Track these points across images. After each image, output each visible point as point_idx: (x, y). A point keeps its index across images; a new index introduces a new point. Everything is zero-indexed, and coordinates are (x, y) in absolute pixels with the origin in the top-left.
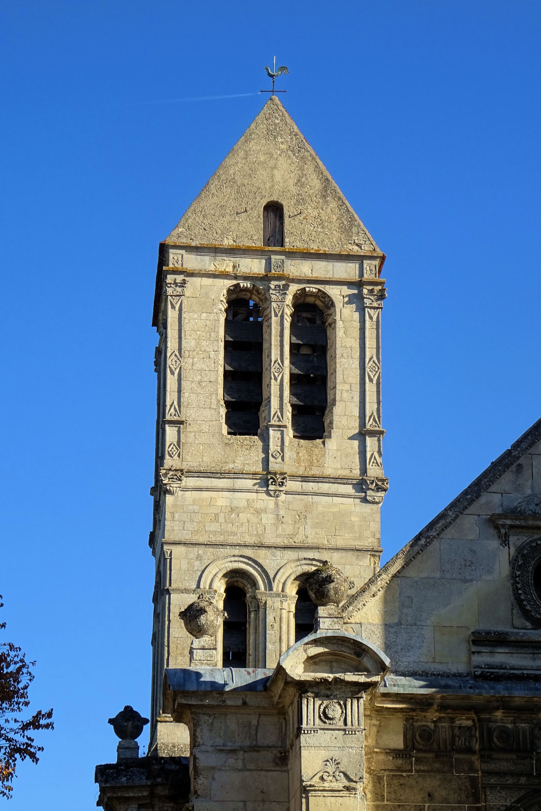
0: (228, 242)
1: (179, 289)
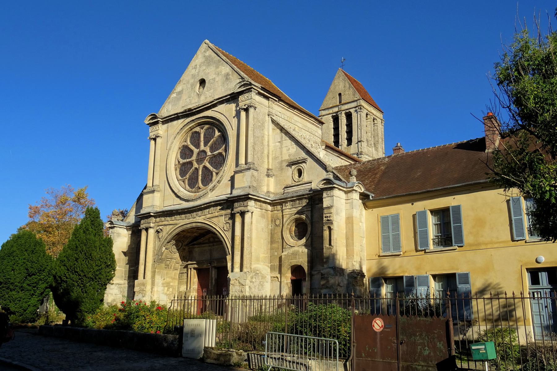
0: (331, 106)
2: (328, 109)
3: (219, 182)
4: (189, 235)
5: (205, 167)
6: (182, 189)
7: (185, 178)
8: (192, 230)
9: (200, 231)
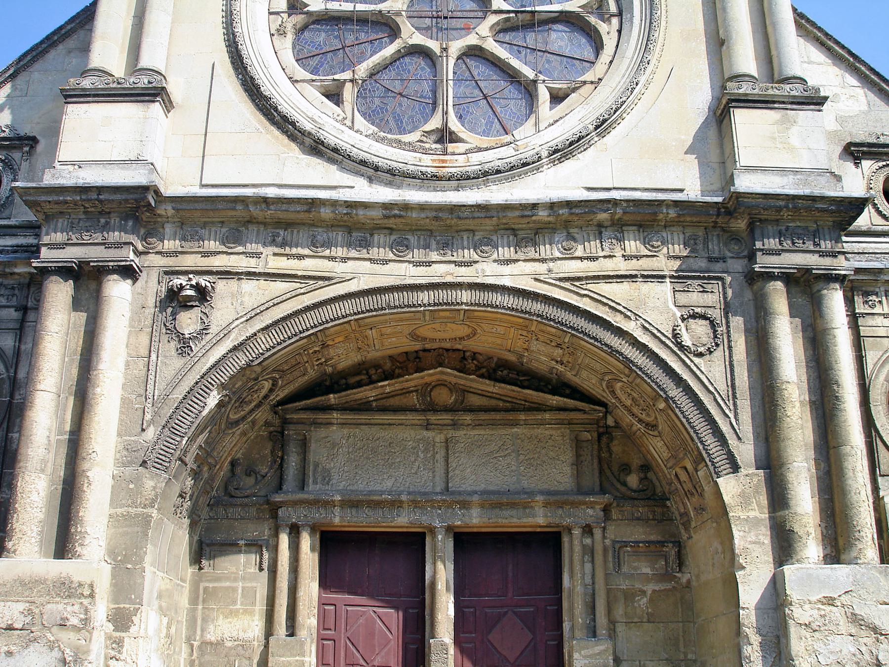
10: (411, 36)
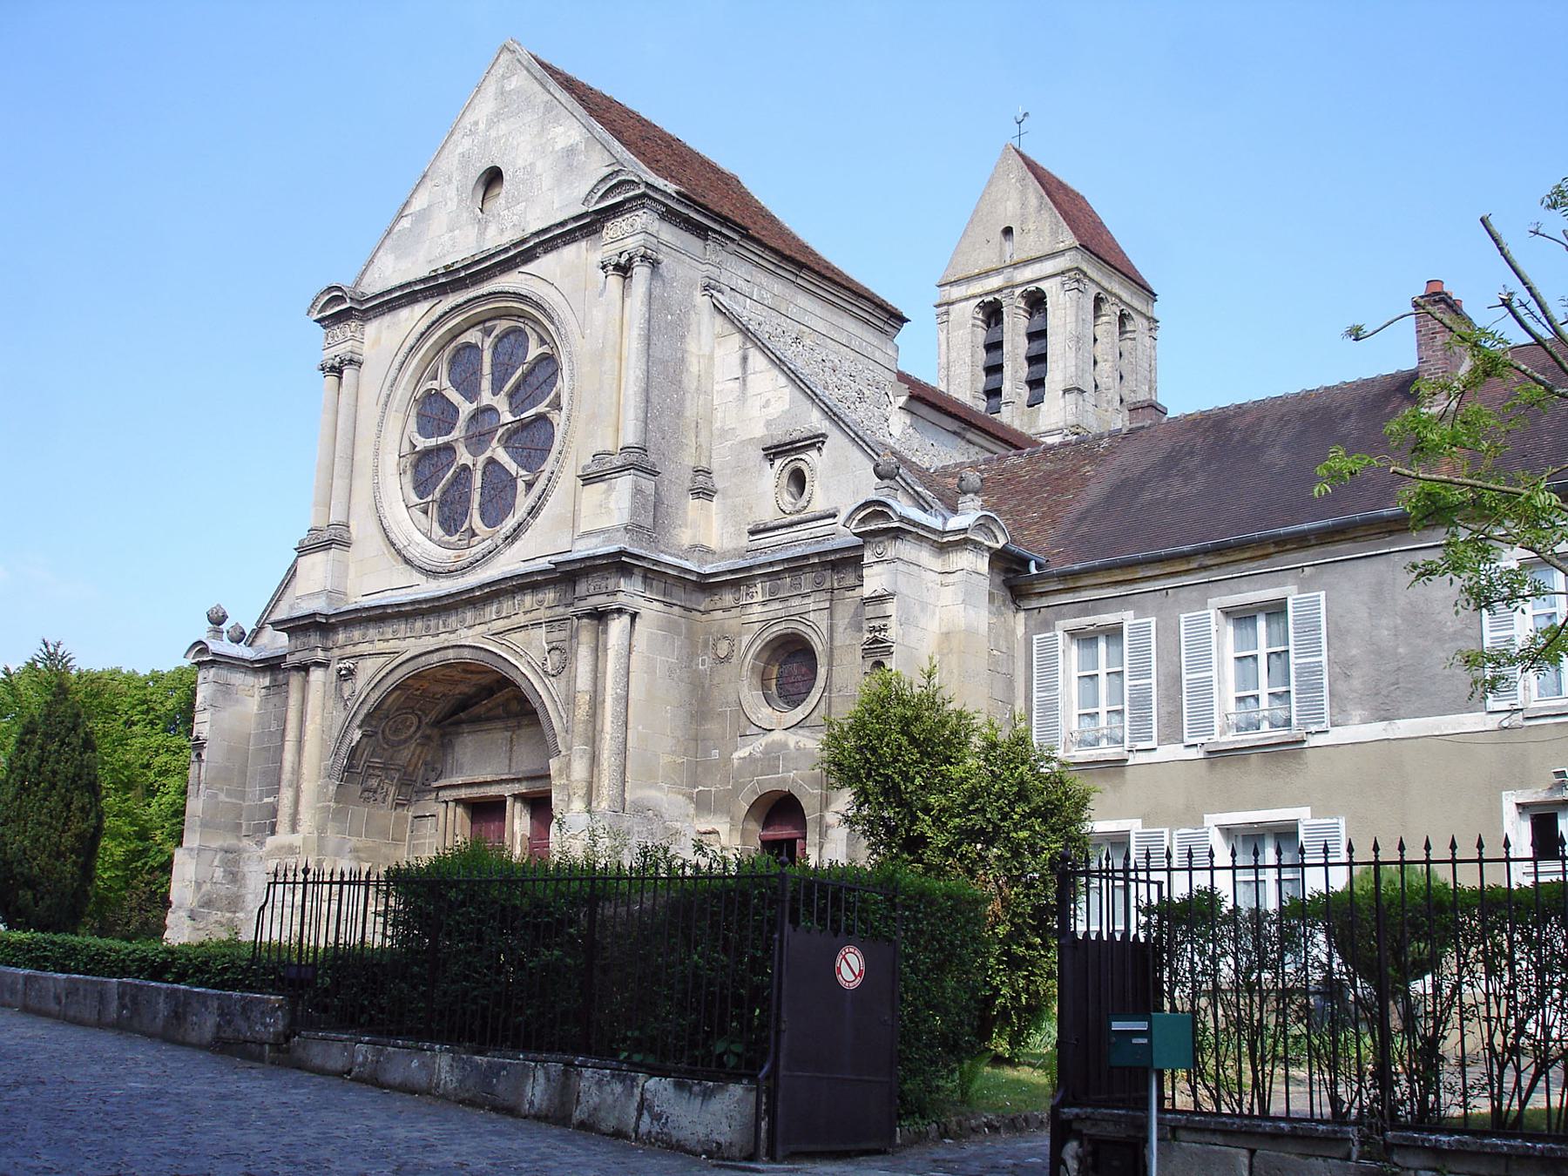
1: (945, 317)
2: (969, 279)
3: (534, 512)
4: (440, 689)
5: (491, 461)
6: (419, 537)
7: (430, 498)
8: (447, 671)
9: (475, 678)
10: (464, 457)
